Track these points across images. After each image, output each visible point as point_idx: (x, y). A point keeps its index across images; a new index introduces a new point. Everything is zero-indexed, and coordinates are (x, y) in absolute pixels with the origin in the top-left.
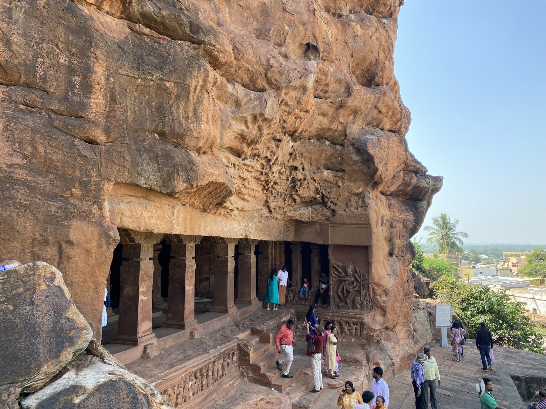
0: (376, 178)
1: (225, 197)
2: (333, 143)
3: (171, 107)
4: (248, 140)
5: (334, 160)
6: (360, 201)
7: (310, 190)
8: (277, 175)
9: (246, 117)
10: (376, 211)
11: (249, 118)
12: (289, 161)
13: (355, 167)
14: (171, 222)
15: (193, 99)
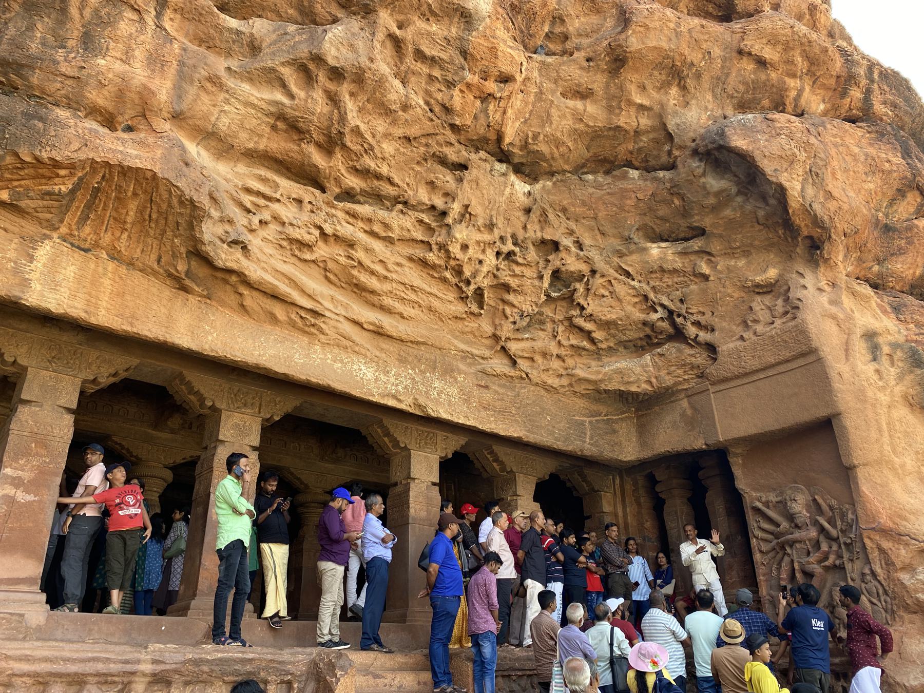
0: (797, 221)
1: (191, 227)
2: (648, 169)
3: (6, 23)
4: (309, 132)
5: (663, 211)
6: (780, 302)
7: (619, 300)
8: (490, 259)
9: (272, 70)
10: (834, 317)
11: (287, 73)
12: (525, 228)
13: (728, 212)
14: (16, 271)
15: (81, 15)
